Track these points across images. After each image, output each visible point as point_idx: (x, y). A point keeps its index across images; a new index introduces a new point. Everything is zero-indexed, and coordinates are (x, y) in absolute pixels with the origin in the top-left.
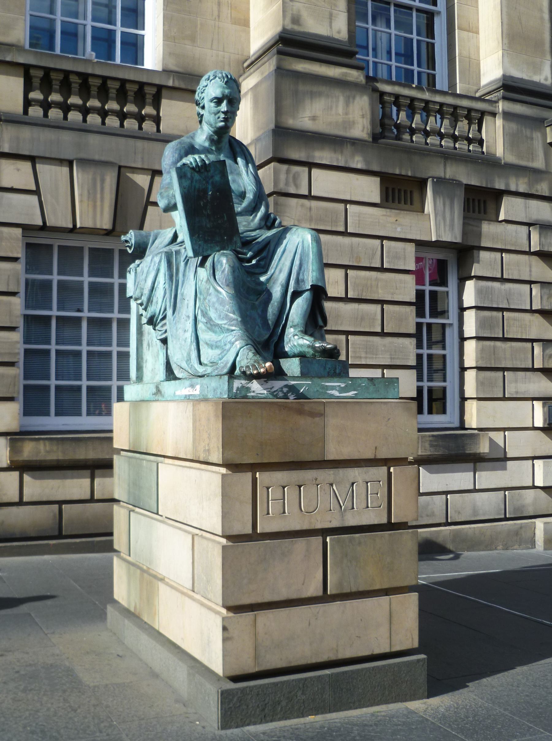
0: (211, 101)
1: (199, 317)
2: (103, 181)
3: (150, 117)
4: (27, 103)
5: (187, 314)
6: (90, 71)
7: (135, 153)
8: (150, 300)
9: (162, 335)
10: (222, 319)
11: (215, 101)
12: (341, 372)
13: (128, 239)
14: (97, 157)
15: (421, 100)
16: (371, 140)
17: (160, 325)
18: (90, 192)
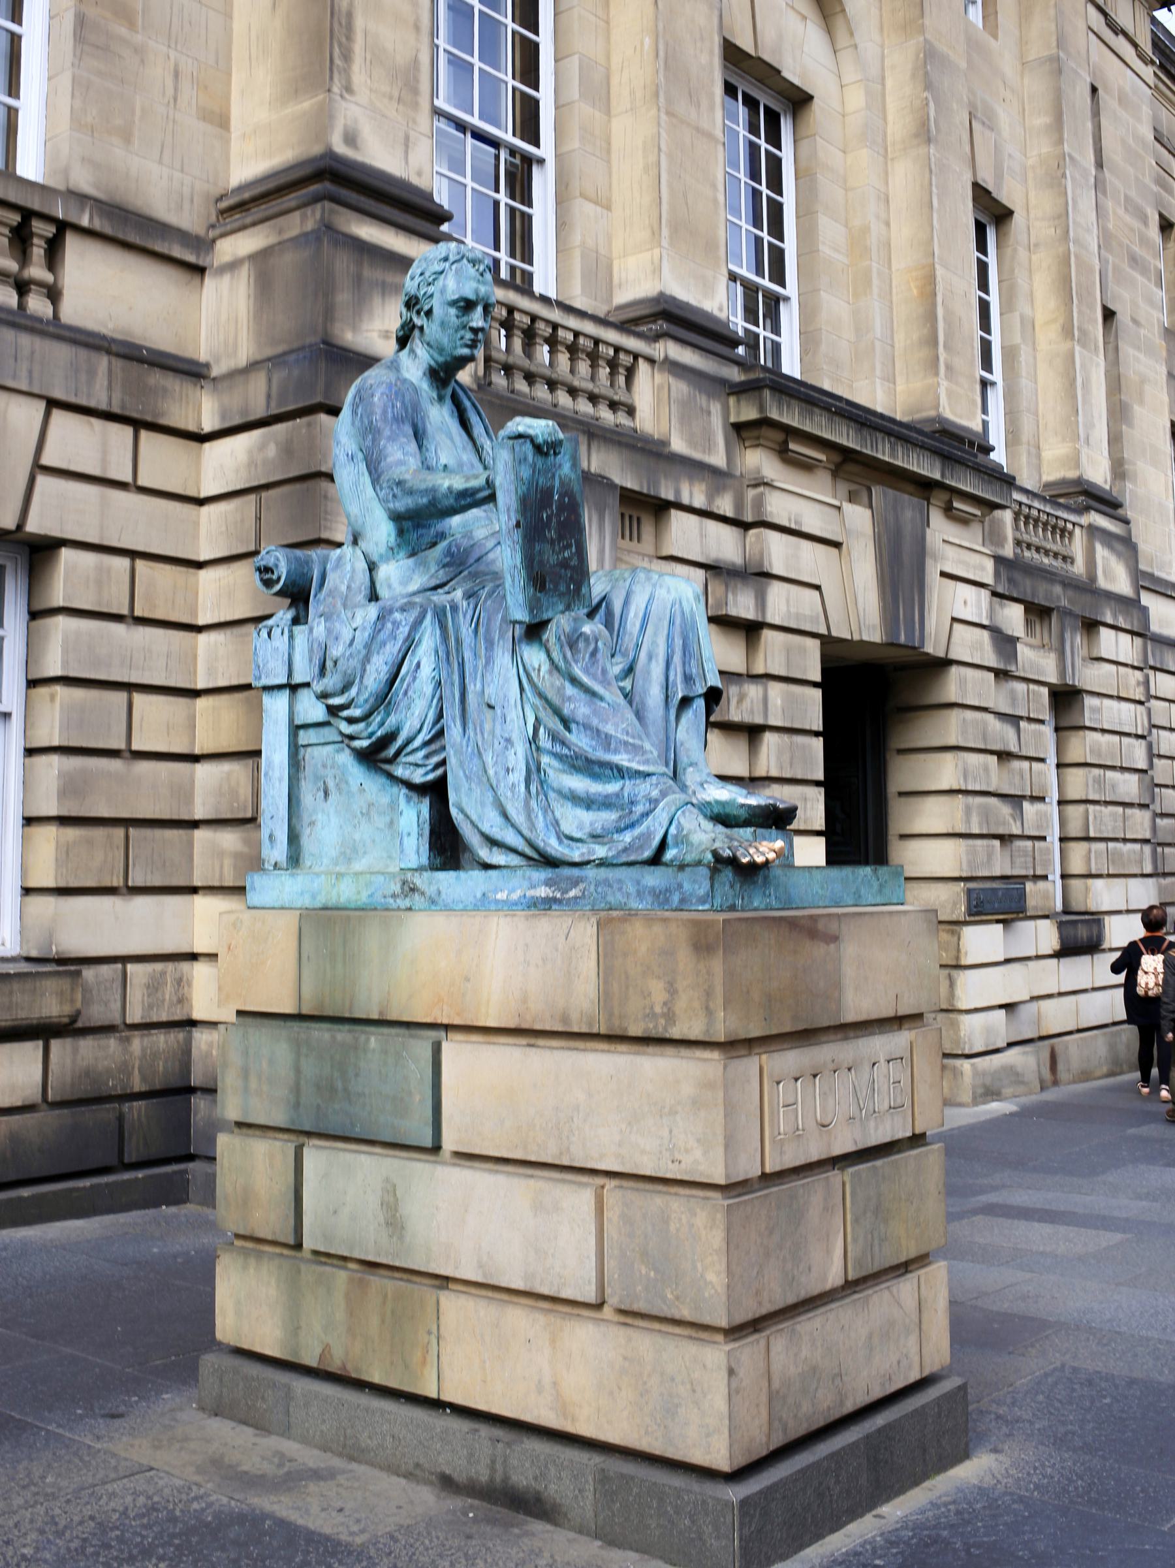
0: (453, 303)
1: (544, 741)
3: (41, 284)
5: (506, 735)
8: (384, 698)
9: (427, 773)
10: (616, 751)
11: (462, 304)
13: (271, 564)
15: (547, 321)
16: (475, 387)
17: (421, 754)
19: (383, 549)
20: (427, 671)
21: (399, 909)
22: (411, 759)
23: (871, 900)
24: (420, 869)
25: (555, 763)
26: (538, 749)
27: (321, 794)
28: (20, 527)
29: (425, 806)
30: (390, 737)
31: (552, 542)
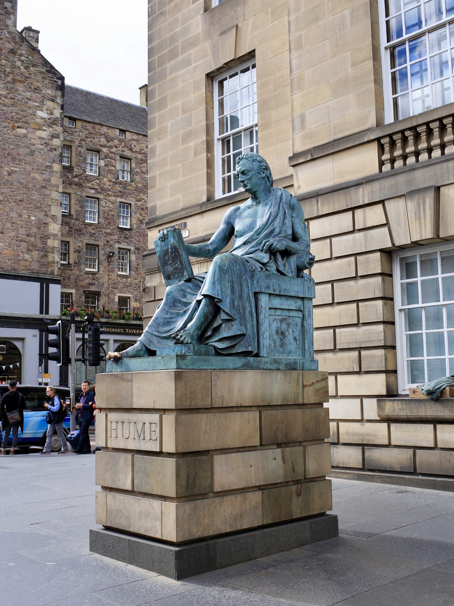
2: (424, 203)
4: (381, 163)
6: (415, 124)
7: (448, 173)
12: (186, 352)
14: (421, 186)
18: (417, 214)
23: (160, 368)
28: (393, 244)
31: (171, 264)
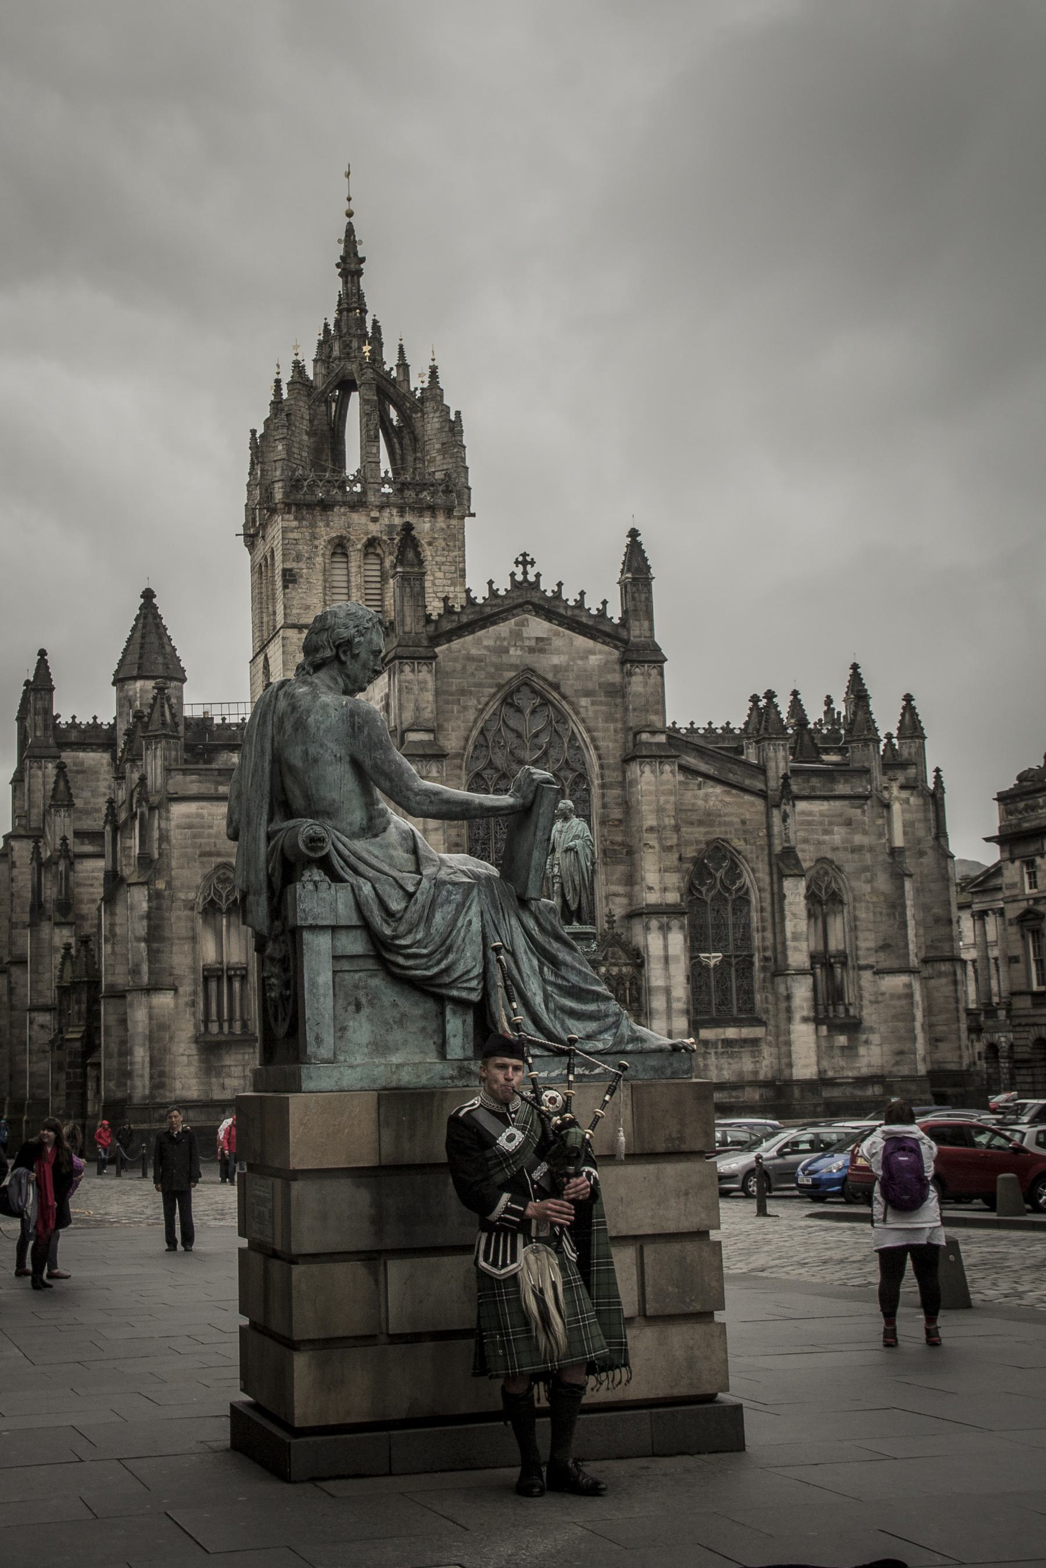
10: (591, 984)
19: (356, 828)
20: (476, 925)
21: (456, 1086)
22: (465, 985)
24: (465, 1059)
25: (555, 991)
26: (544, 980)
27: (354, 1007)
29: (470, 1019)
30: (447, 970)
